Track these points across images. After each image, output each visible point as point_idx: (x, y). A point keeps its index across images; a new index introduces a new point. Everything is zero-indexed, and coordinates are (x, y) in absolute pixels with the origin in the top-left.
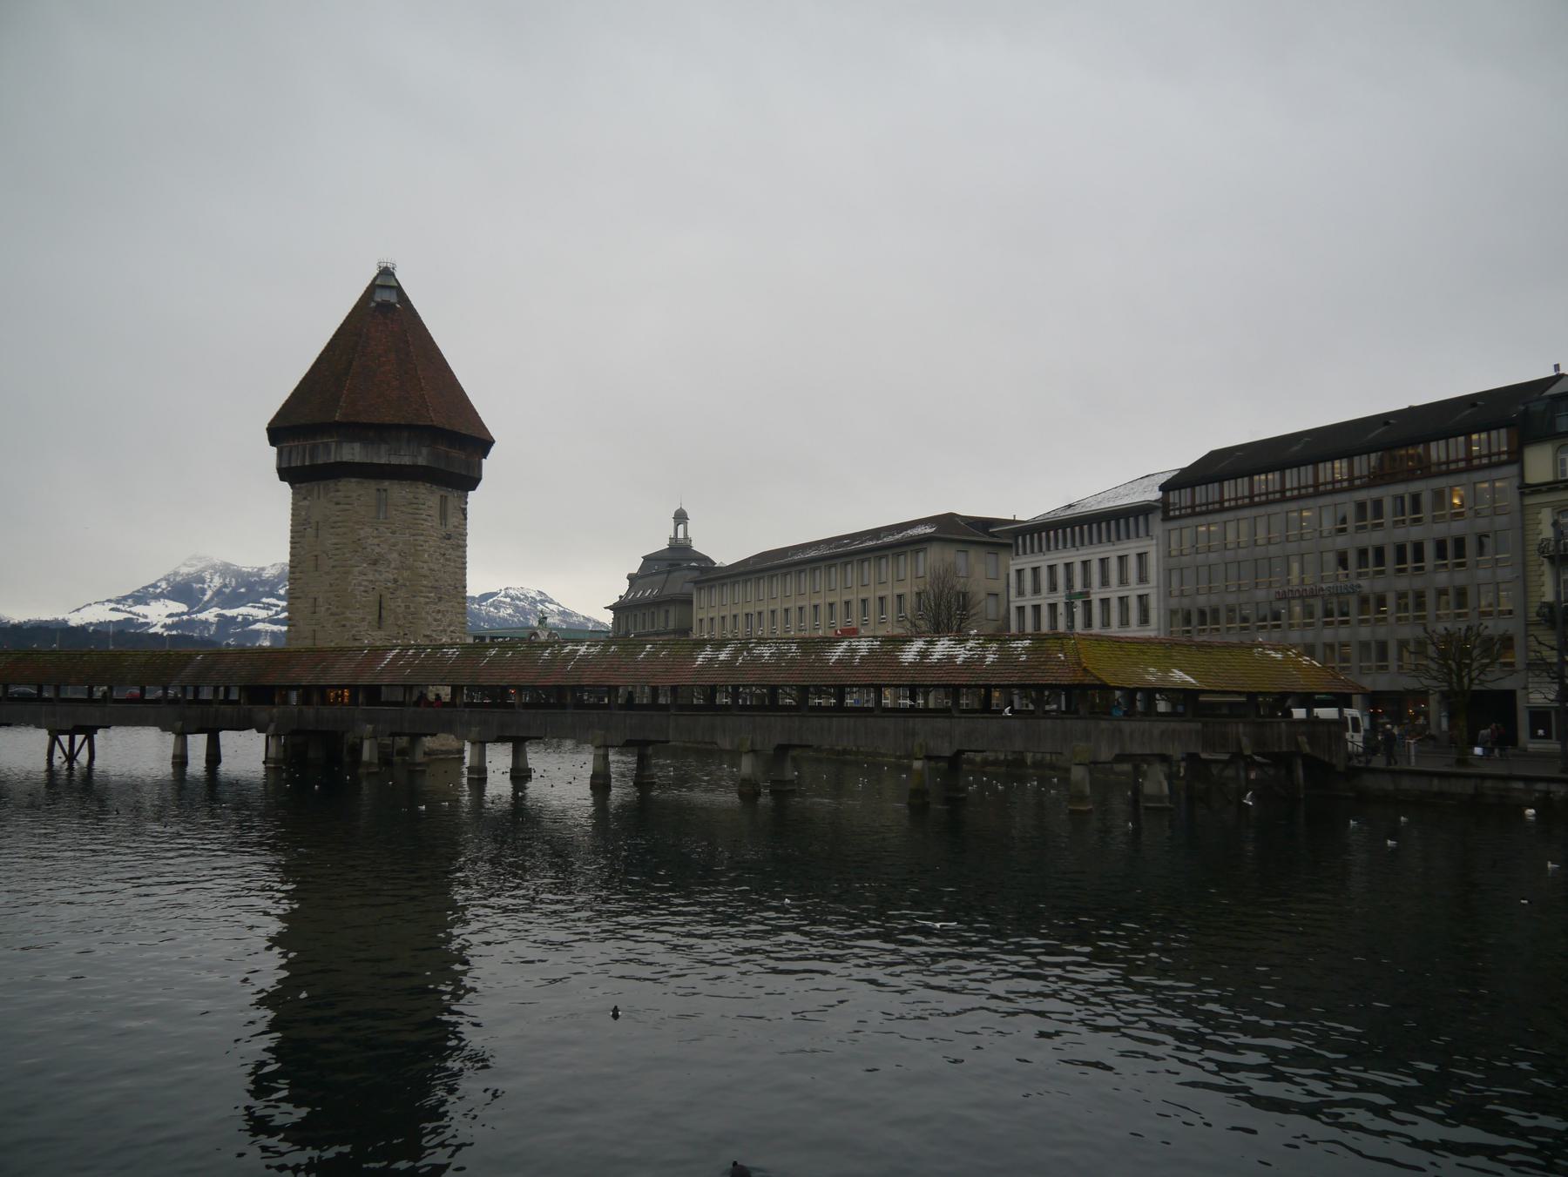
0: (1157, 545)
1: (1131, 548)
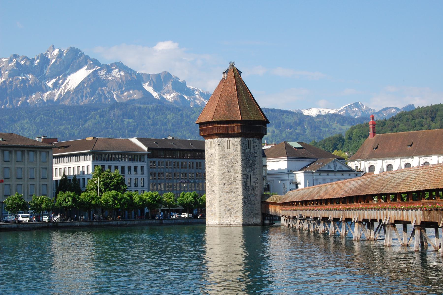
1: (139, 164)
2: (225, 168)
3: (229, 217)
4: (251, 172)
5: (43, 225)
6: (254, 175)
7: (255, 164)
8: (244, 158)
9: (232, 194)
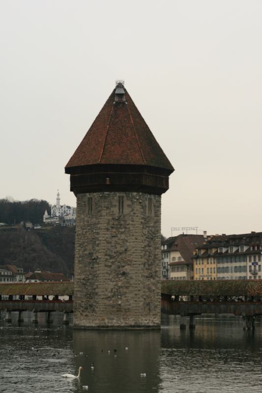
2: (145, 240)
3: (146, 315)
9: (152, 280)
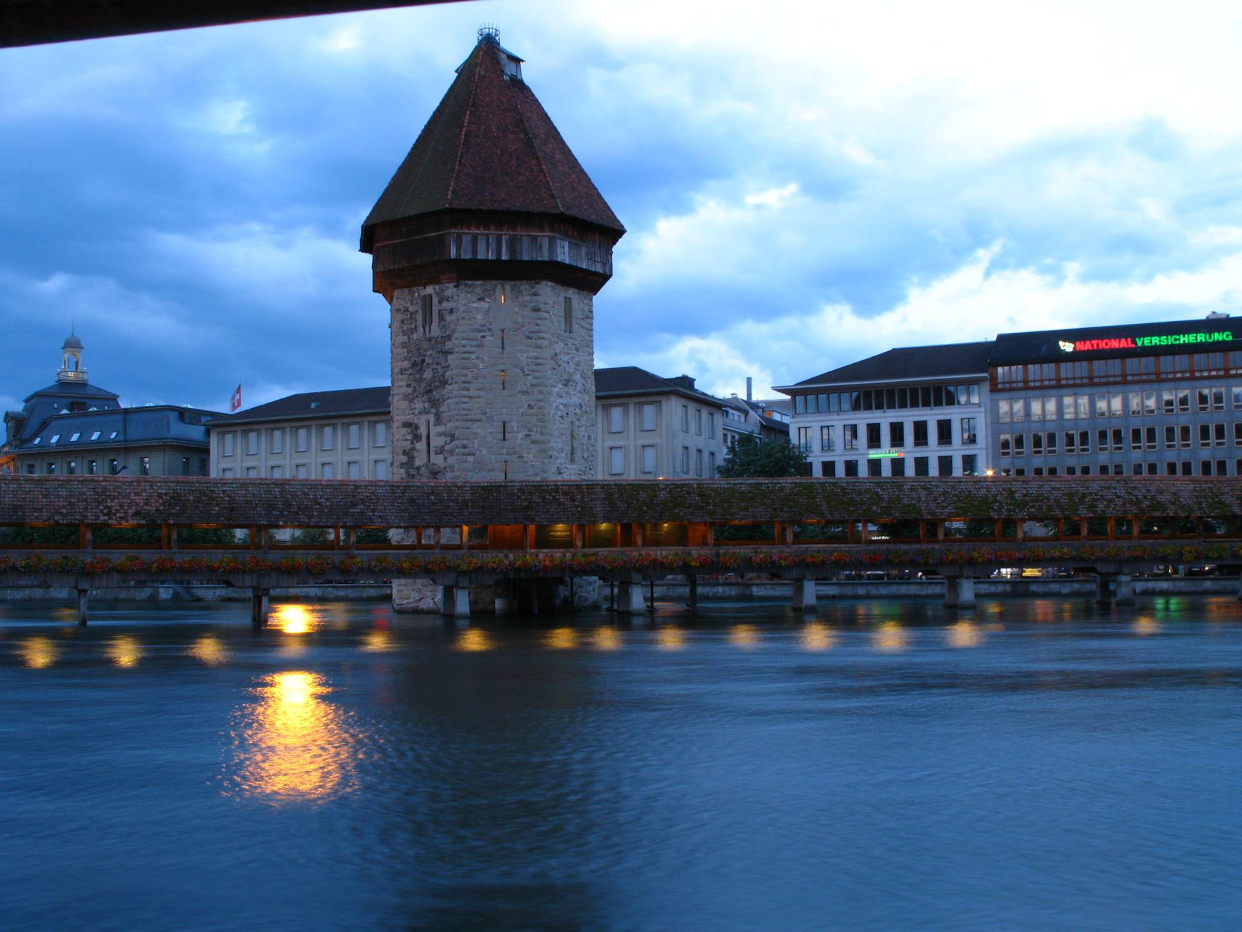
0: (985, 412)
4: (427, 413)
5: (382, 593)
6: (439, 424)
7: (444, 383)
8: (406, 364)
